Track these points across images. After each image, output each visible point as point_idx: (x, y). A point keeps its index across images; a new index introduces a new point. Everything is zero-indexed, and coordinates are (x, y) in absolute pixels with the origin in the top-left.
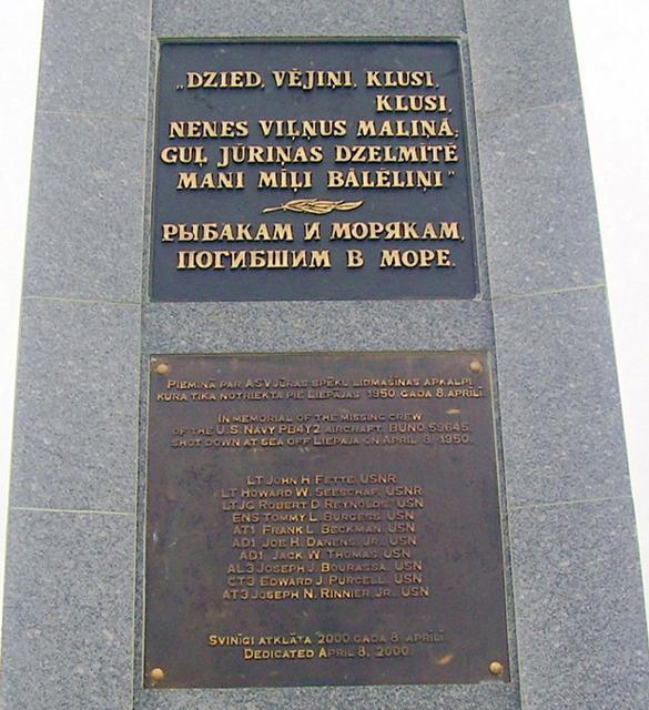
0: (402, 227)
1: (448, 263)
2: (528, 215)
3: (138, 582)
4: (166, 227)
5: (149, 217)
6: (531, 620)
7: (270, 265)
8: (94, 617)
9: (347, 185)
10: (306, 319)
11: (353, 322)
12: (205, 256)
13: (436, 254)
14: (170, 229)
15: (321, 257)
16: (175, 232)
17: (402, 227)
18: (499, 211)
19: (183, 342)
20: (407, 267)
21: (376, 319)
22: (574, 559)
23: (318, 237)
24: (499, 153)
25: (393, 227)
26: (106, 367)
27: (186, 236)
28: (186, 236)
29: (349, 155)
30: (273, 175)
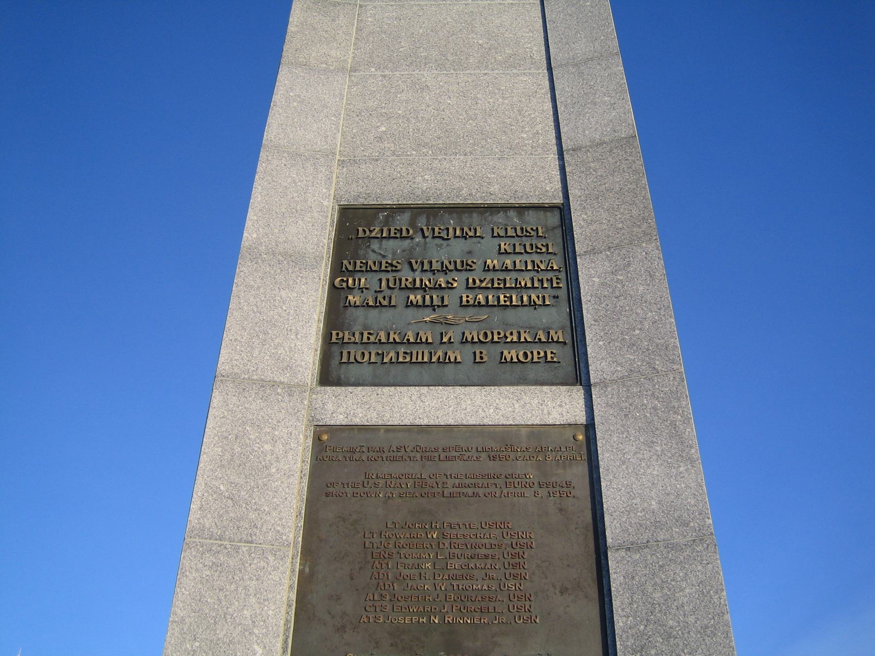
0: (519, 333)
1: (555, 360)
2: (618, 322)
3: (289, 606)
4: (334, 333)
5: (322, 325)
6: (629, 643)
7: (414, 360)
8: (247, 633)
9: (476, 303)
10: (441, 400)
11: (478, 402)
12: (363, 354)
13: (545, 353)
14: (338, 334)
15: (455, 355)
16: (341, 336)
17: (519, 333)
18: (595, 321)
19: (341, 416)
20: (523, 363)
21: (497, 401)
22: (666, 591)
23: (452, 340)
24: (594, 279)
25: (511, 334)
26: (277, 433)
27: (350, 339)
28: (350, 339)
29: (368, 232)
30: (419, 297)
